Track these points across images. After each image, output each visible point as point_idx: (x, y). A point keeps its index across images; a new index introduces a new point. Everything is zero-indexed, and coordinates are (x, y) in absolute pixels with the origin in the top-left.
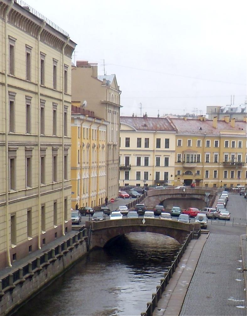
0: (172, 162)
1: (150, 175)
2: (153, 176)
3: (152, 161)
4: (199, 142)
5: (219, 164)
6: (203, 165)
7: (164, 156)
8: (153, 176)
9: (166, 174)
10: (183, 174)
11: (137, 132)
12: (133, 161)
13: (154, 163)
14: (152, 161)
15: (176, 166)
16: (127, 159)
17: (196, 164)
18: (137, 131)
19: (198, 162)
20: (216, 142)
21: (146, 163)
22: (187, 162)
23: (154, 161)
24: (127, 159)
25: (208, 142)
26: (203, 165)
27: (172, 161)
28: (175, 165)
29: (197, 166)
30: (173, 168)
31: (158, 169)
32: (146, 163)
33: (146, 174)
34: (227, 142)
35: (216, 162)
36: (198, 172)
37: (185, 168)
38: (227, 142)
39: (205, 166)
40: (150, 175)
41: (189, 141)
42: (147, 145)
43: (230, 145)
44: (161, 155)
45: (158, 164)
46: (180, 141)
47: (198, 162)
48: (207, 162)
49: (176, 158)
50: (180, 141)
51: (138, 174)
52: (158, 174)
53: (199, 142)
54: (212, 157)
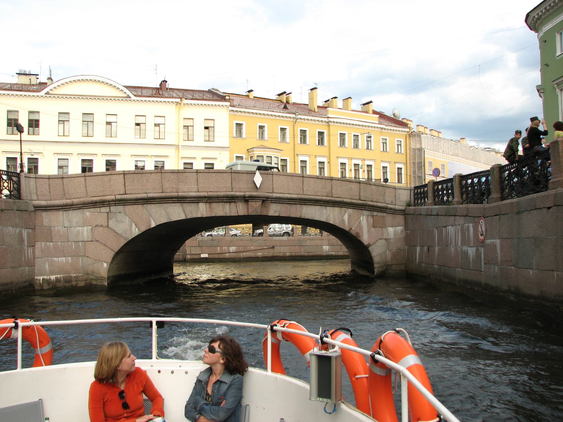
11: (134, 100)
18: (133, 98)
46: (239, 125)
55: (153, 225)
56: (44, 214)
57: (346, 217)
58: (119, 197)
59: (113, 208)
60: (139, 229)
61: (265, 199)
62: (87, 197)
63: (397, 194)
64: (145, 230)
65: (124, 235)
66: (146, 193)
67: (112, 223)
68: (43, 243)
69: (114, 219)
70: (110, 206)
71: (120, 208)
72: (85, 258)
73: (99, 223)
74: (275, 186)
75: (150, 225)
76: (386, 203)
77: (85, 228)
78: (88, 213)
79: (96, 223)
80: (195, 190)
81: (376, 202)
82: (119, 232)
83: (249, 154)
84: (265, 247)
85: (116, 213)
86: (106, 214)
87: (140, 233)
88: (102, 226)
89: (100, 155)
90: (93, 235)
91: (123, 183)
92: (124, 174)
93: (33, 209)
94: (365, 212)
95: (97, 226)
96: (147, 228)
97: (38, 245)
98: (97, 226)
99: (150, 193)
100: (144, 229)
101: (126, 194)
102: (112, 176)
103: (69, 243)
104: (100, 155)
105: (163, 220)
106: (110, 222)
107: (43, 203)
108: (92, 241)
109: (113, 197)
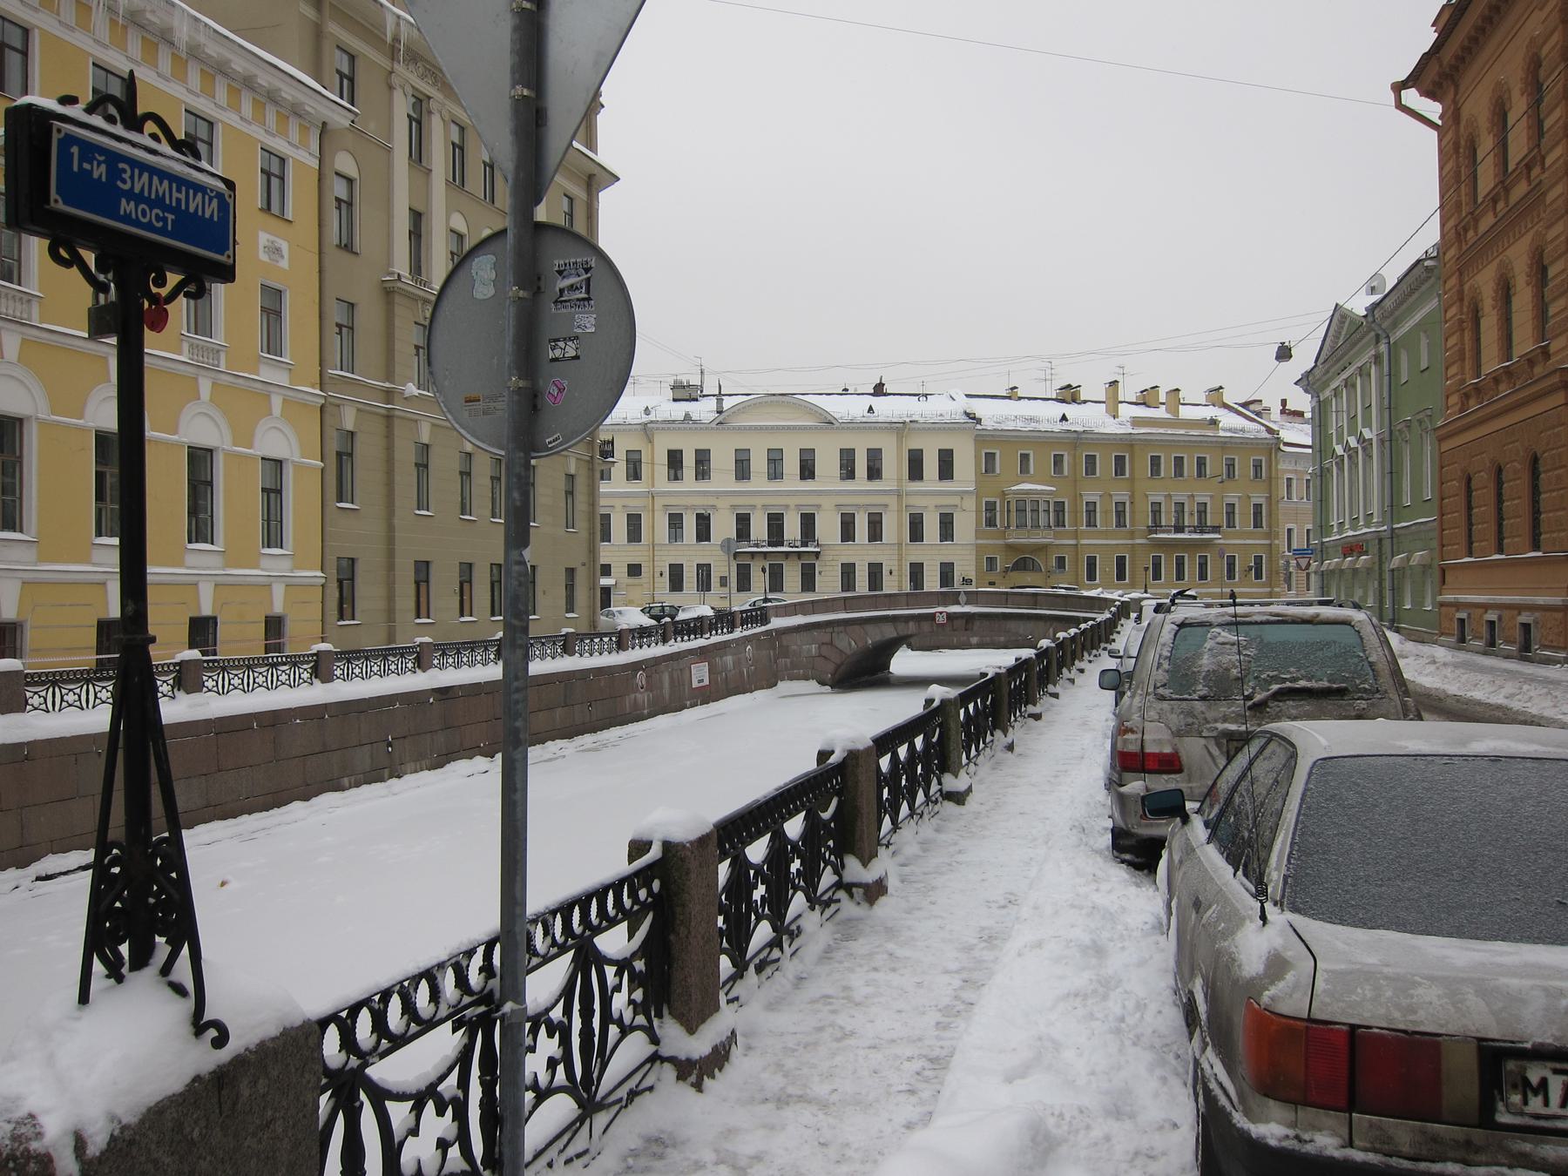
0: (965, 526)
1: (891, 573)
3: (894, 527)
4: (1058, 460)
5: (1132, 535)
8: (900, 576)
9: (947, 572)
12: (829, 529)
14: (894, 527)
15: (980, 542)
16: (808, 522)
20: (1120, 461)
21: (875, 533)
23: (900, 525)
24: (808, 522)
25: (1091, 460)
27: (965, 526)
31: (915, 553)
32: (875, 533)
33: (875, 572)
34: (1155, 461)
36: (1061, 562)
37: (1011, 548)
38: (1155, 461)
40: (891, 573)
41: (1025, 457)
42: (874, 473)
43: (1167, 468)
45: (916, 533)
46: (990, 457)
49: (978, 511)
50: (990, 457)
51: (848, 571)
52: (917, 571)
53: (1058, 460)
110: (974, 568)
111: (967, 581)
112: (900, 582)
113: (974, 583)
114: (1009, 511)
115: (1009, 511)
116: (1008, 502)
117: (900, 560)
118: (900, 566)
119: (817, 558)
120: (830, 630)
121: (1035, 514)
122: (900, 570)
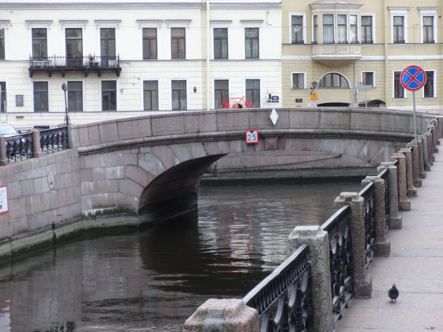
1: (195, 90)
2: (205, 93)
6: (384, 54)
7: (242, 21)
8: (205, 93)
10: (314, 83)
13: (204, 48)
15: (285, 57)
17: (359, 47)
19: (368, 41)
22: (325, 43)
23: (204, 41)
26: (384, 54)
28: (283, 54)
29: (364, 58)
30: (277, 63)
35: (429, 41)
36: (369, 76)
39: (390, 57)
40: (195, 90)
44: (230, 21)
47: (368, 41)
48: (399, 41)
49: (284, 27)
54: (415, 27)
55: (178, 162)
56: (86, 158)
57: (365, 150)
58: (147, 139)
59: (142, 150)
60: (164, 167)
61: (281, 136)
62: (119, 140)
63: (423, 123)
64: (170, 168)
65: (152, 173)
66: (170, 134)
67: (142, 163)
68: (86, 182)
69: (142, 159)
70: (139, 148)
71: (148, 149)
72: (119, 193)
73: (130, 163)
74: (291, 122)
75: (175, 162)
76: (411, 133)
77: (118, 167)
78: (120, 154)
79: (128, 163)
80: (215, 129)
81: (399, 132)
82: (147, 170)
83: (313, 11)
84: (329, 156)
85: (145, 154)
86: (136, 155)
87: (166, 170)
88: (132, 165)
89: (91, 22)
90: (125, 174)
91: (150, 126)
92: (151, 118)
93: (78, 155)
94: (387, 143)
95: (128, 165)
96: (172, 166)
97: (83, 183)
98: (128, 165)
99: (174, 134)
100: (169, 166)
101: (152, 136)
102: (140, 120)
103: (106, 181)
104: (91, 22)
105: (186, 158)
106: (140, 162)
107: (84, 149)
108: (124, 178)
109: (141, 140)
110: (280, 85)
111: (273, 99)
112: (205, 99)
113: (280, 100)
114: (316, 26)
115: (316, 26)
116: (315, 17)
117: (205, 77)
118: (205, 83)
119: (118, 75)
120: (135, 151)
121: (329, 29)
122: (205, 88)
